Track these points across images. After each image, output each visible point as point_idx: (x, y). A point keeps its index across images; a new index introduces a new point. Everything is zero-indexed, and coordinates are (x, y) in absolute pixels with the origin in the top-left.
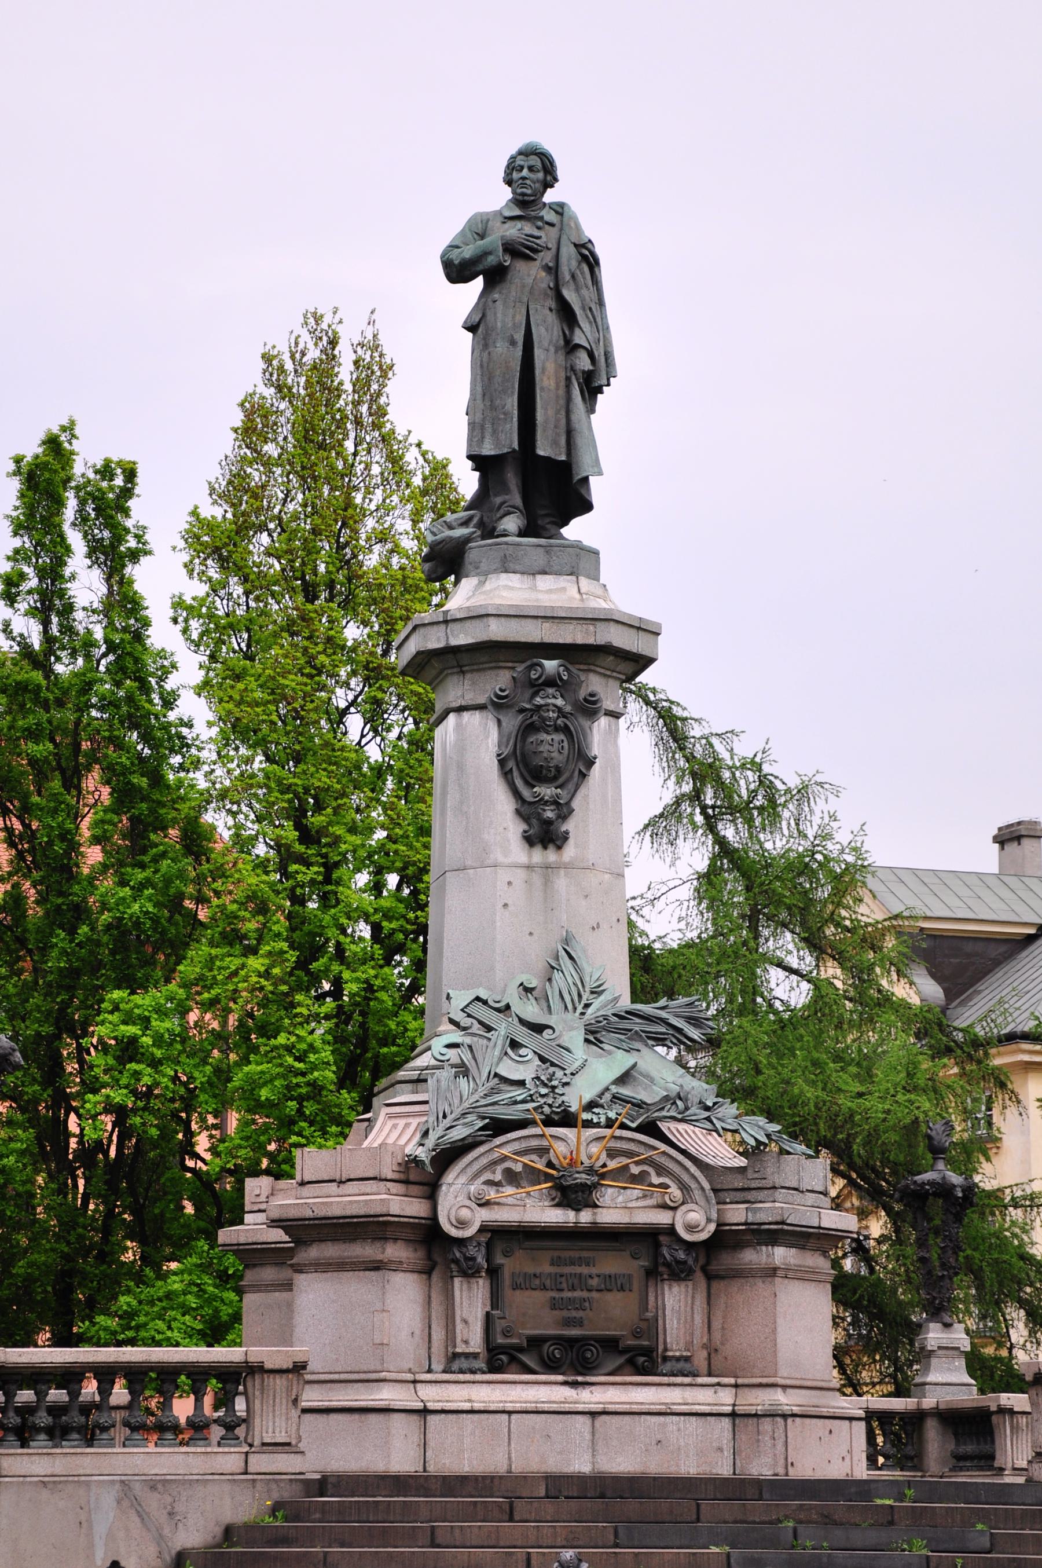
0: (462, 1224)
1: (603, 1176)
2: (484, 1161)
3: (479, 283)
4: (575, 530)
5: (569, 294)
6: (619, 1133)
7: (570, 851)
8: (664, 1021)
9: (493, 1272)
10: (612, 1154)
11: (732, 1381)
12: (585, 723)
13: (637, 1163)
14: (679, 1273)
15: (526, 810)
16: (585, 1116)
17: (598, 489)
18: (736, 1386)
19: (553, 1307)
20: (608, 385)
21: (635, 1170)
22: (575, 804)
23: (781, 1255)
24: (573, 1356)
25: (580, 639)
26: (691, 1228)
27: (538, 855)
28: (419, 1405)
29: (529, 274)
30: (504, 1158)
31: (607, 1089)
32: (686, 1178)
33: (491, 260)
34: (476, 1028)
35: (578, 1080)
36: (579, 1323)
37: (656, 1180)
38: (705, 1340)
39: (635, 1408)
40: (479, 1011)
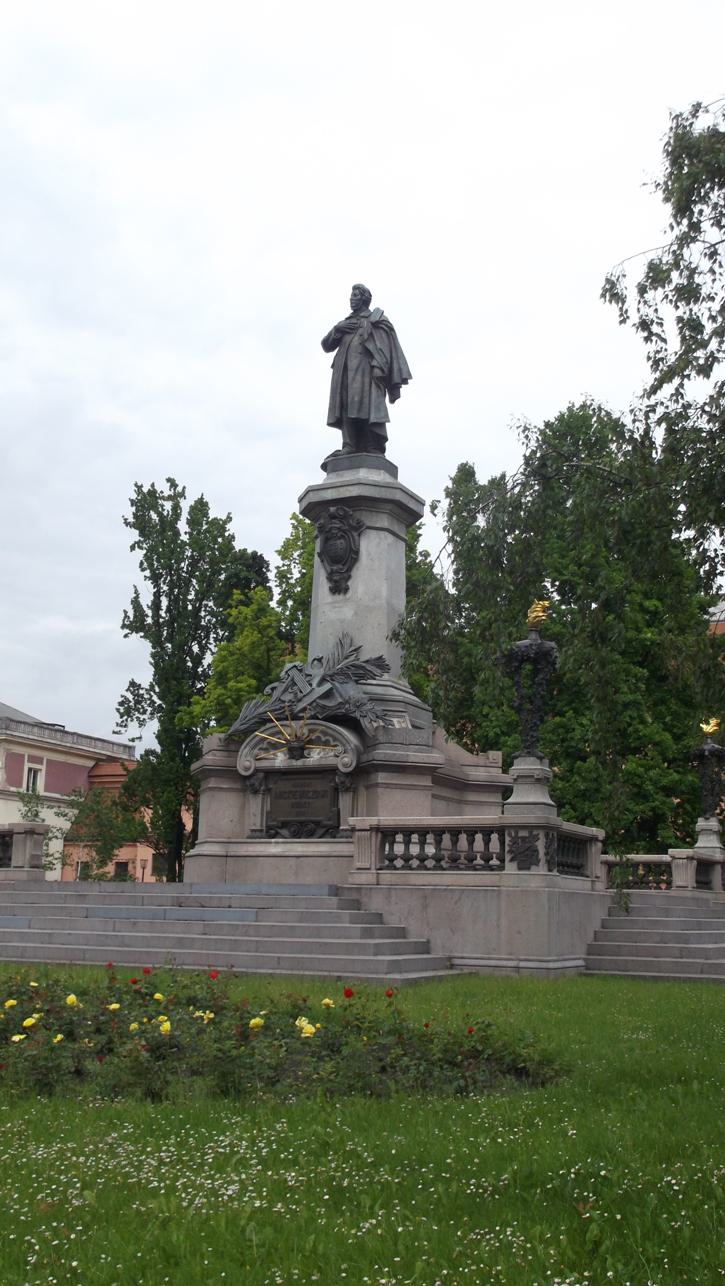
0: (247, 769)
1: (311, 742)
2: (257, 739)
6: (312, 721)
12: (355, 534)
14: (347, 790)
15: (330, 578)
16: (301, 715)
17: (391, 429)
19: (293, 807)
20: (406, 383)
21: (323, 739)
22: (354, 573)
23: (382, 777)
24: (303, 830)
25: (348, 494)
26: (345, 765)
27: (340, 597)
28: (224, 854)
29: (355, 340)
30: (264, 739)
31: (314, 701)
33: (331, 339)
35: (305, 699)
37: (332, 743)
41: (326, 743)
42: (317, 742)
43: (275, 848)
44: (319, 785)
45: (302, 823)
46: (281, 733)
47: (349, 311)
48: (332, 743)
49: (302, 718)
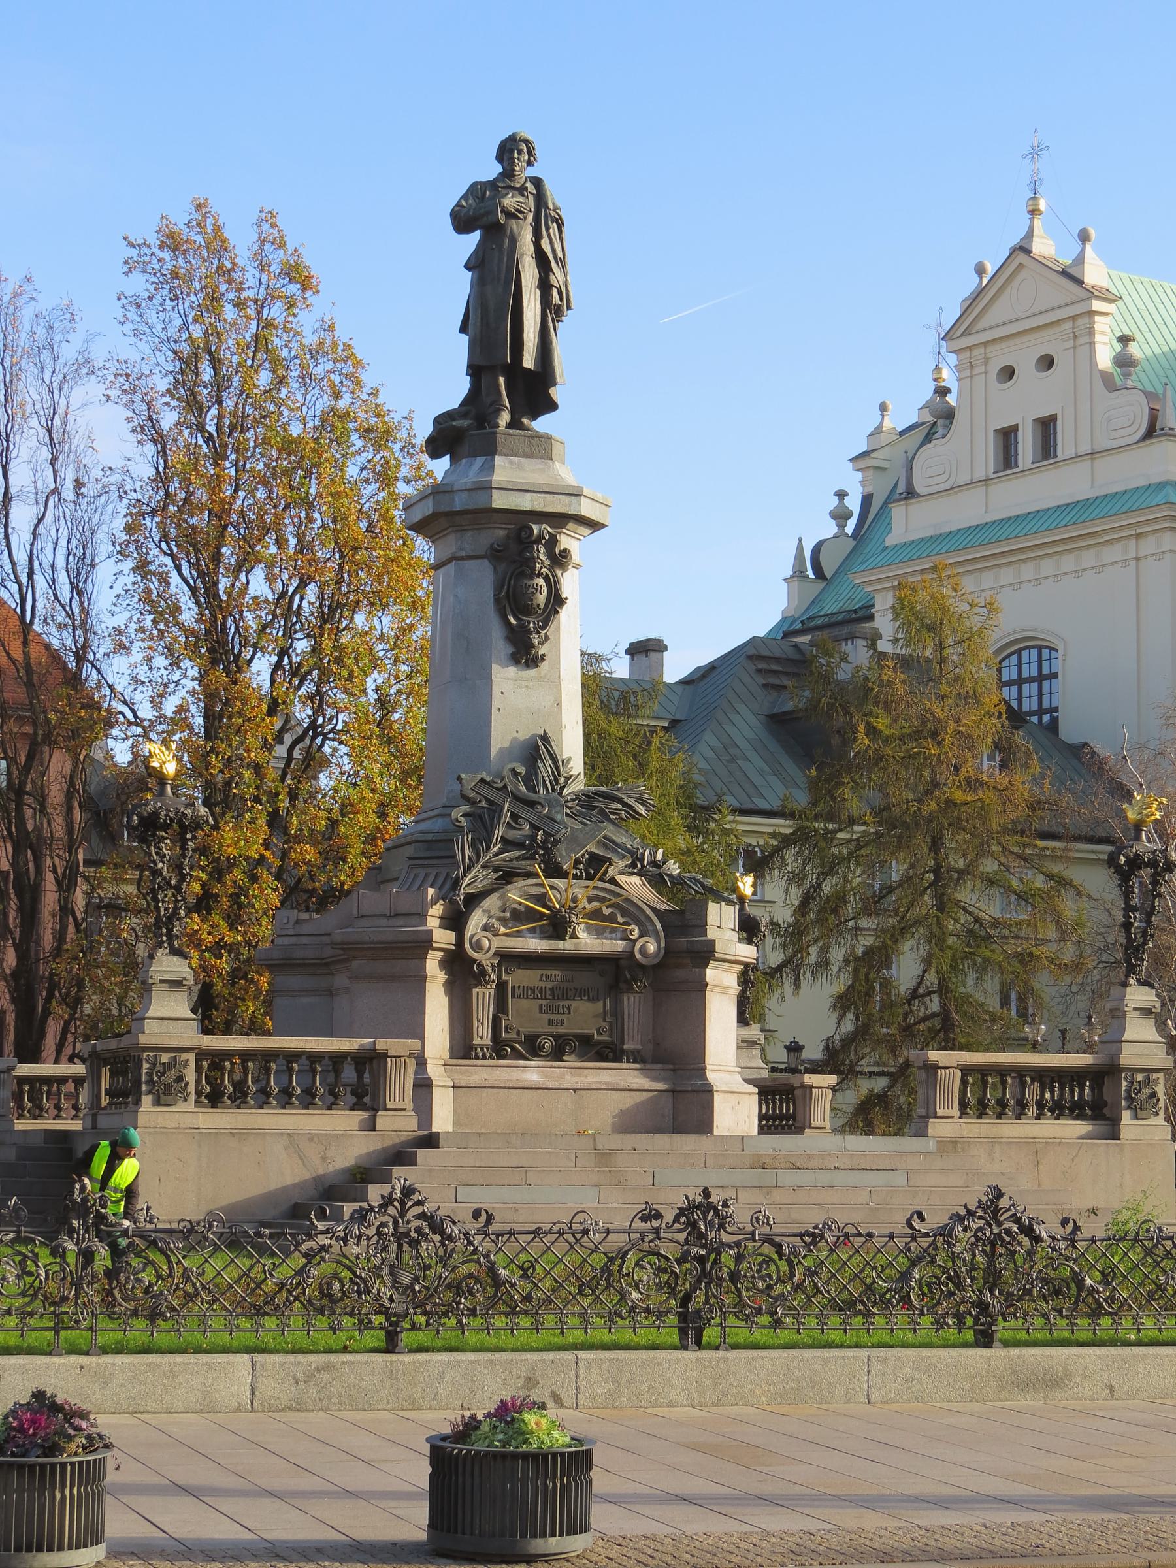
3: (476, 236)
4: (542, 424)
5: (545, 244)
7: (544, 666)
8: (620, 801)
9: (501, 987)
10: (590, 899)
11: (671, 1067)
13: (607, 907)
18: (674, 1070)
21: (607, 911)
32: (642, 918)
34: (484, 804)
36: (561, 1023)
38: (650, 1037)
39: (604, 1087)
40: (485, 791)
41: (611, 918)
42: (596, 914)
43: (532, 1072)
44: (585, 978)
45: (557, 1037)
46: (541, 899)
47: (493, 170)
48: (620, 919)
49: (575, 877)
